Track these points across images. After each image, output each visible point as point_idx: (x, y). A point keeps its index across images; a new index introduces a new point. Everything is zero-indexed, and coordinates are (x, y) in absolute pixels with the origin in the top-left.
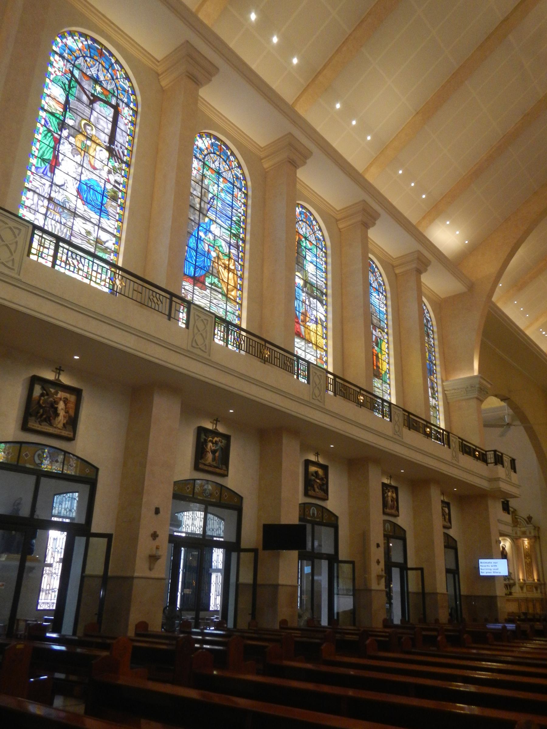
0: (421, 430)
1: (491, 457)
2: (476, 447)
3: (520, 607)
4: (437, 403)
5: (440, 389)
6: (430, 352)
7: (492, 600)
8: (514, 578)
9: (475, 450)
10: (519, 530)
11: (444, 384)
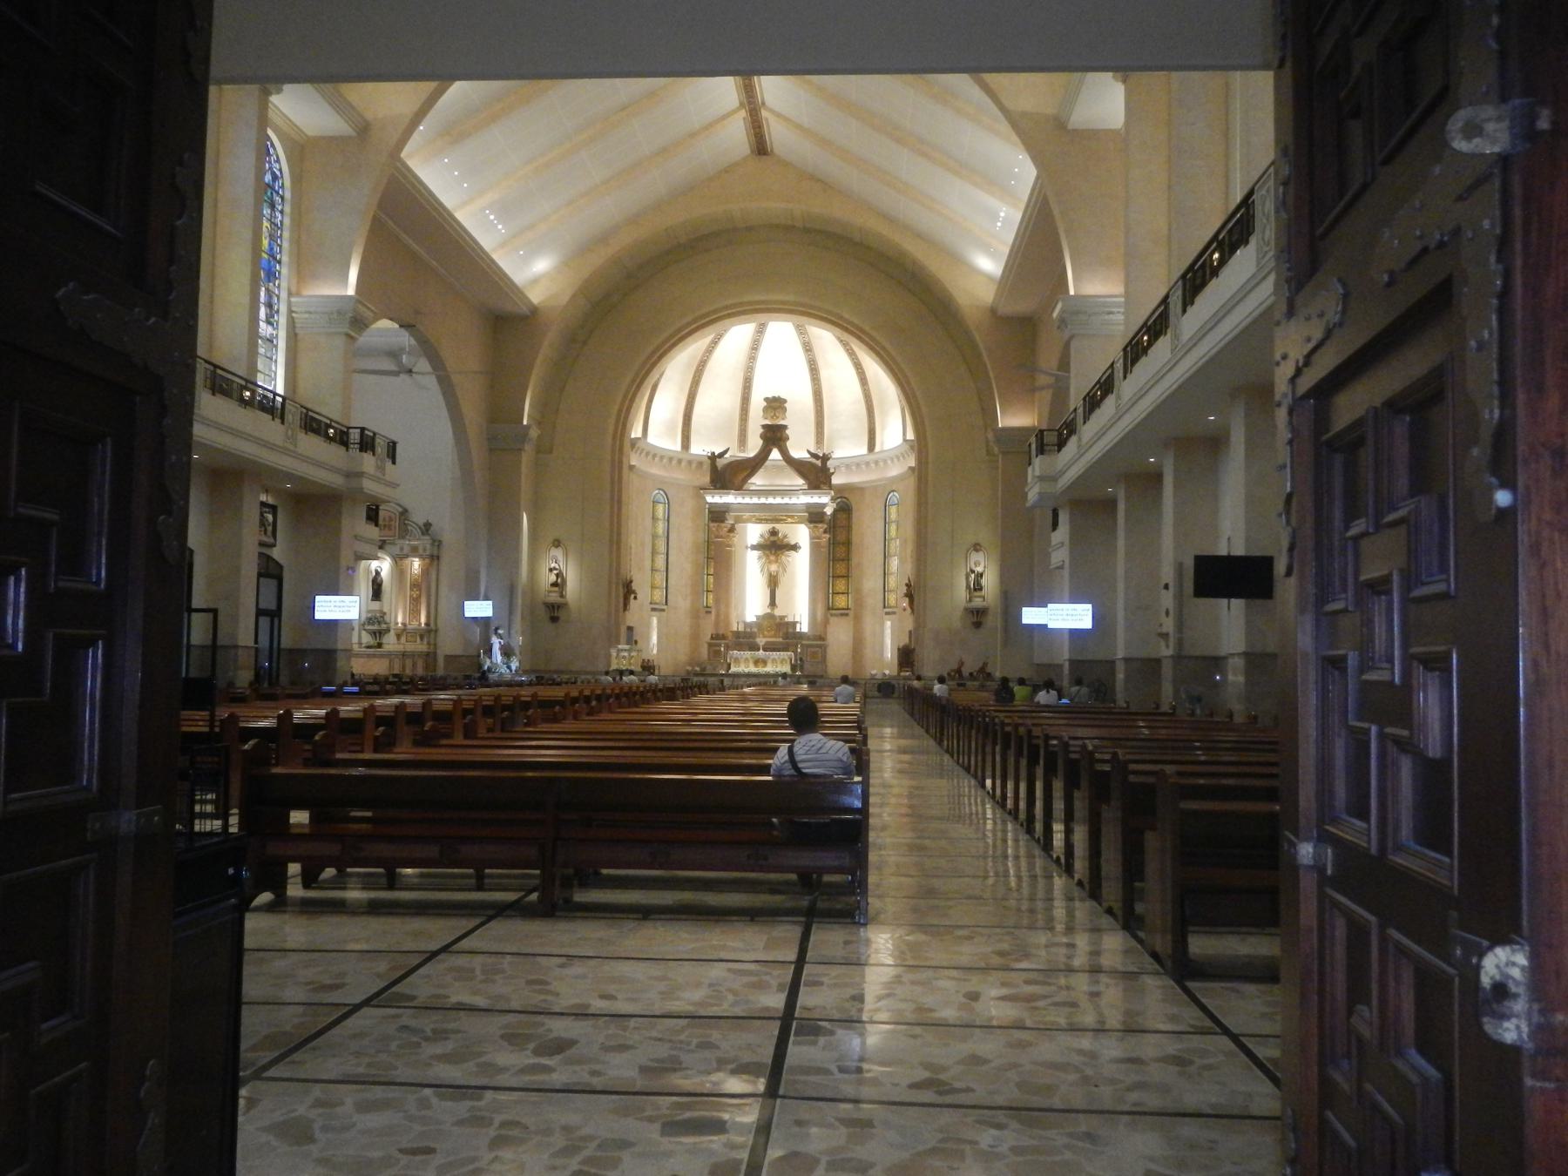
0: (235, 395)
1: (355, 436)
2: (331, 420)
3: (391, 667)
4: (275, 332)
5: (283, 308)
6: (272, 237)
7: (327, 657)
8: (388, 620)
9: (329, 426)
10: (406, 544)
11: (293, 299)
